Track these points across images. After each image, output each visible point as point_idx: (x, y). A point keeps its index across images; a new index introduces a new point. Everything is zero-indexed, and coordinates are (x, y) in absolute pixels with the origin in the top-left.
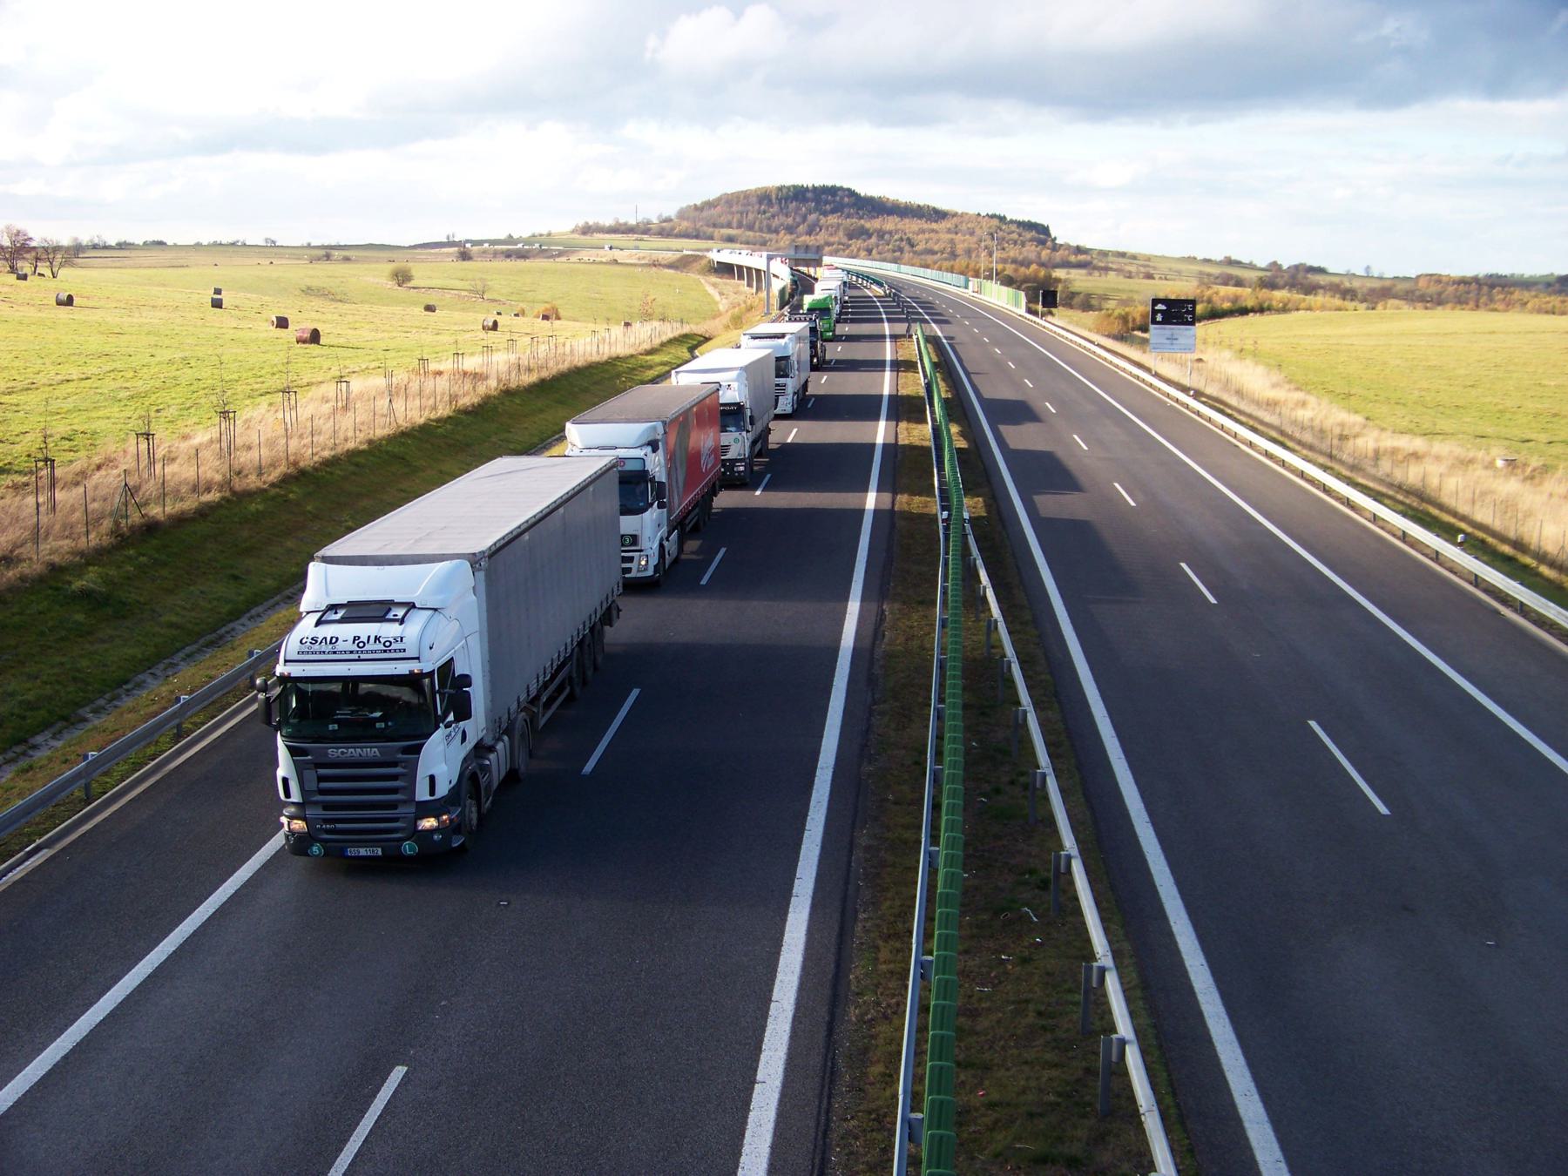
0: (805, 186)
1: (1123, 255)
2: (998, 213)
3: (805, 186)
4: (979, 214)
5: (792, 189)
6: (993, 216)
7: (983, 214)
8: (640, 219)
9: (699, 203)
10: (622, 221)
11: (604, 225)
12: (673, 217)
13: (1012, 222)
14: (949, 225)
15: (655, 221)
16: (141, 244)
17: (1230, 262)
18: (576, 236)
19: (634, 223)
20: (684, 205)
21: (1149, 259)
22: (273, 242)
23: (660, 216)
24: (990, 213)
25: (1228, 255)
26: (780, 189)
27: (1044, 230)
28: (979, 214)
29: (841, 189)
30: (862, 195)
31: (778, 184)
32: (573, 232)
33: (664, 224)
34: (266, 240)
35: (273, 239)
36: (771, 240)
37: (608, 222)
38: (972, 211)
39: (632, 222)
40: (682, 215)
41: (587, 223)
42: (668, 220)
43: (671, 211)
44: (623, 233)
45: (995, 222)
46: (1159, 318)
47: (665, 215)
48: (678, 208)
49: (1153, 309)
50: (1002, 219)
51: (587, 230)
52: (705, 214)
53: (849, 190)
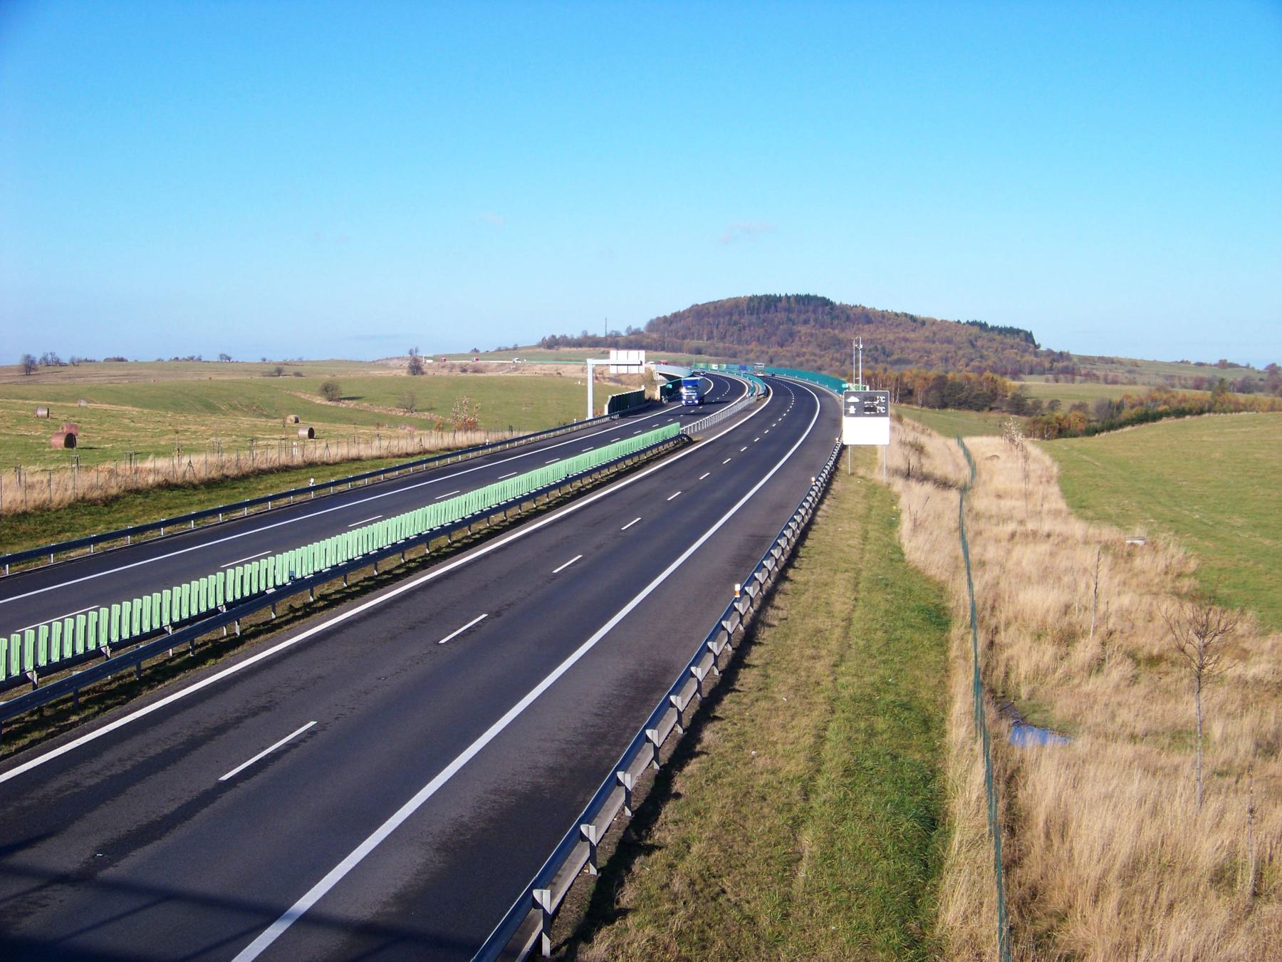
0: (778, 295)
1: (1111, 361)
2: (978, 320)
3: (778, 295)
4: (959, 322)
5: (764, 299)
6: (974, 324)
7: (963, 321)
8: (608, 333)
9: (668, 314)
10: (590, 334)
11: (572, 338)
12: (642, 330)
13: (993, 329)
14: (927, 334)
15: (624, 334)
16: (102, 360)
17: (1223, 364)
18: (543, 350)
19: (603, 336)
20: (654, 317)
21: (1135, 364)
22: (229, 359)
23: (629, 328)
24: (970, 321)
25: (1223, 358)
26: (752, 299)
27: (1029, 337)
28: (959, 322)
29: (815, 298)
30: (838, 303)
31: (749, 295)
32: (539, 346)
33: (632, 337)
34: (222, 356)
35: (229, 355)
36: (741, 352)
37: (576, 334)
38: (952, 318)
39: (601, 334)
40: (653, 325)
41: (554, 337)
42: (637, 332)
43: (641, 324)
44: (590, 346)
45: (975, 330)
46: (852, 410)
47: (634, 327)
48: (648, 320)
49: (846, 403)
50: (983, 326)
51: (553, 343)
52: (674, 326)
53: (824, 299)
